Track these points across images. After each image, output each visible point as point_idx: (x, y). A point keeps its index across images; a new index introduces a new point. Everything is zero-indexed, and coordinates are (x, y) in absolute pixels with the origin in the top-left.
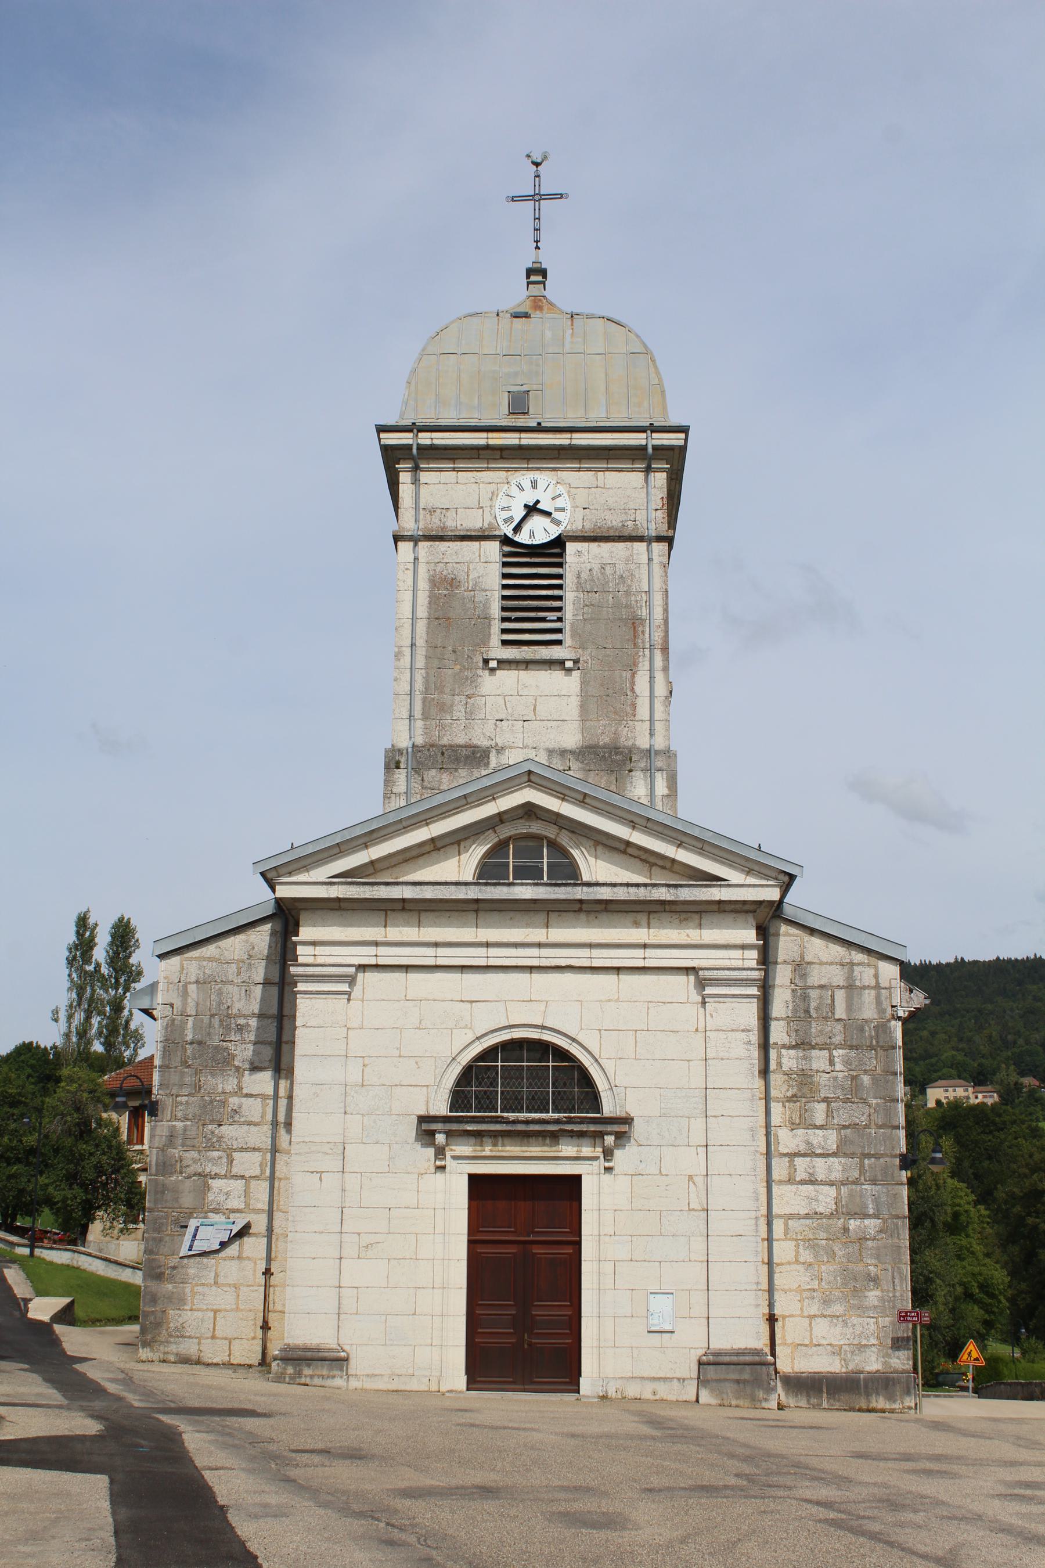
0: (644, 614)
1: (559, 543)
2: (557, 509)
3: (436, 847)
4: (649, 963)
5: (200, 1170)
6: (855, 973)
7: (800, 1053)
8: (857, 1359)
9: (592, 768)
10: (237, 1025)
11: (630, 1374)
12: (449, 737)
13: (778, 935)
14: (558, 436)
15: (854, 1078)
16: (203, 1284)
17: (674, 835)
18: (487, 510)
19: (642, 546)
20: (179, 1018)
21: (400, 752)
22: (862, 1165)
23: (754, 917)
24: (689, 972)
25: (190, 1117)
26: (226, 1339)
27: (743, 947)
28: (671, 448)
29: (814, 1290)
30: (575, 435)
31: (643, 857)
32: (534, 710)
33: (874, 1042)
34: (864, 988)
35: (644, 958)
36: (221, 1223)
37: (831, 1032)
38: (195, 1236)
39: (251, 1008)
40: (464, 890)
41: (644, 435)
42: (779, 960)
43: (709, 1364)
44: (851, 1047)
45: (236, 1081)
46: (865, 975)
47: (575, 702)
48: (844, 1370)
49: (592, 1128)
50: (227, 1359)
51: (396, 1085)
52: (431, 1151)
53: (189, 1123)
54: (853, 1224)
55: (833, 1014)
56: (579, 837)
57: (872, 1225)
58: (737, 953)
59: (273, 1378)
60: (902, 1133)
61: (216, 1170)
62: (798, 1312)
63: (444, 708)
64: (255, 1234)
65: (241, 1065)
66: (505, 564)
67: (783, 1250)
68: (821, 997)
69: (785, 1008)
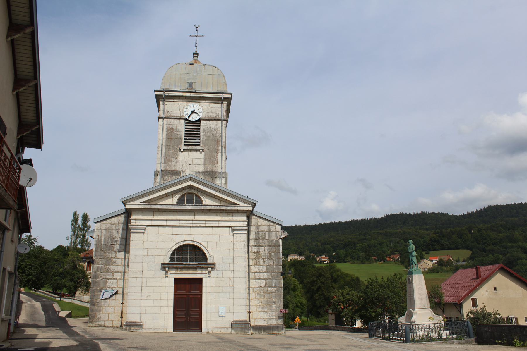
1: (199, 121)
2: (199, 112)
3: (167, 196)
4: (220, 225)
5: (105, 277)
6: (271, 228)
7: (257, 247)
8: (270, 322)
9: (207, 176)
11: (214, 327)
13: (252, 218)
14: (200, 94)
15: (270, 253)
16: (106, 307)
17: (227, 193)
19: (220, 122)
20: (100, 238)
21: (158, 171)
22: (272, 275)
23: (246, 214)
25: (103, 264)
26: (111, 320)
27: (243, 221)
28: (228, 98)
29: (260, 305)
30: (204, 94)
33: (275, 245)
34: (273, 231)
36: (110, 291)
37: (264, 242)
38: (103, 294)
41: (221, 95)
43: (234, 324)
44: (269, 246)
45: (115, 255)
46: (273, 228)
47: (202, 160)
48: (267, 324)
49: (205, 266)
50: (112, 325)
52: (164, 272)
53: (102, 265)
54: (269, 289)
55: (265, 238)
57: (274, 289)
58: (242, 223)
60: (281, 267)
61: (109, 277)
63: (169, 161)
64: (119, 294)
66: (186, 125)
67: (252, 296)
68: (262, 234)
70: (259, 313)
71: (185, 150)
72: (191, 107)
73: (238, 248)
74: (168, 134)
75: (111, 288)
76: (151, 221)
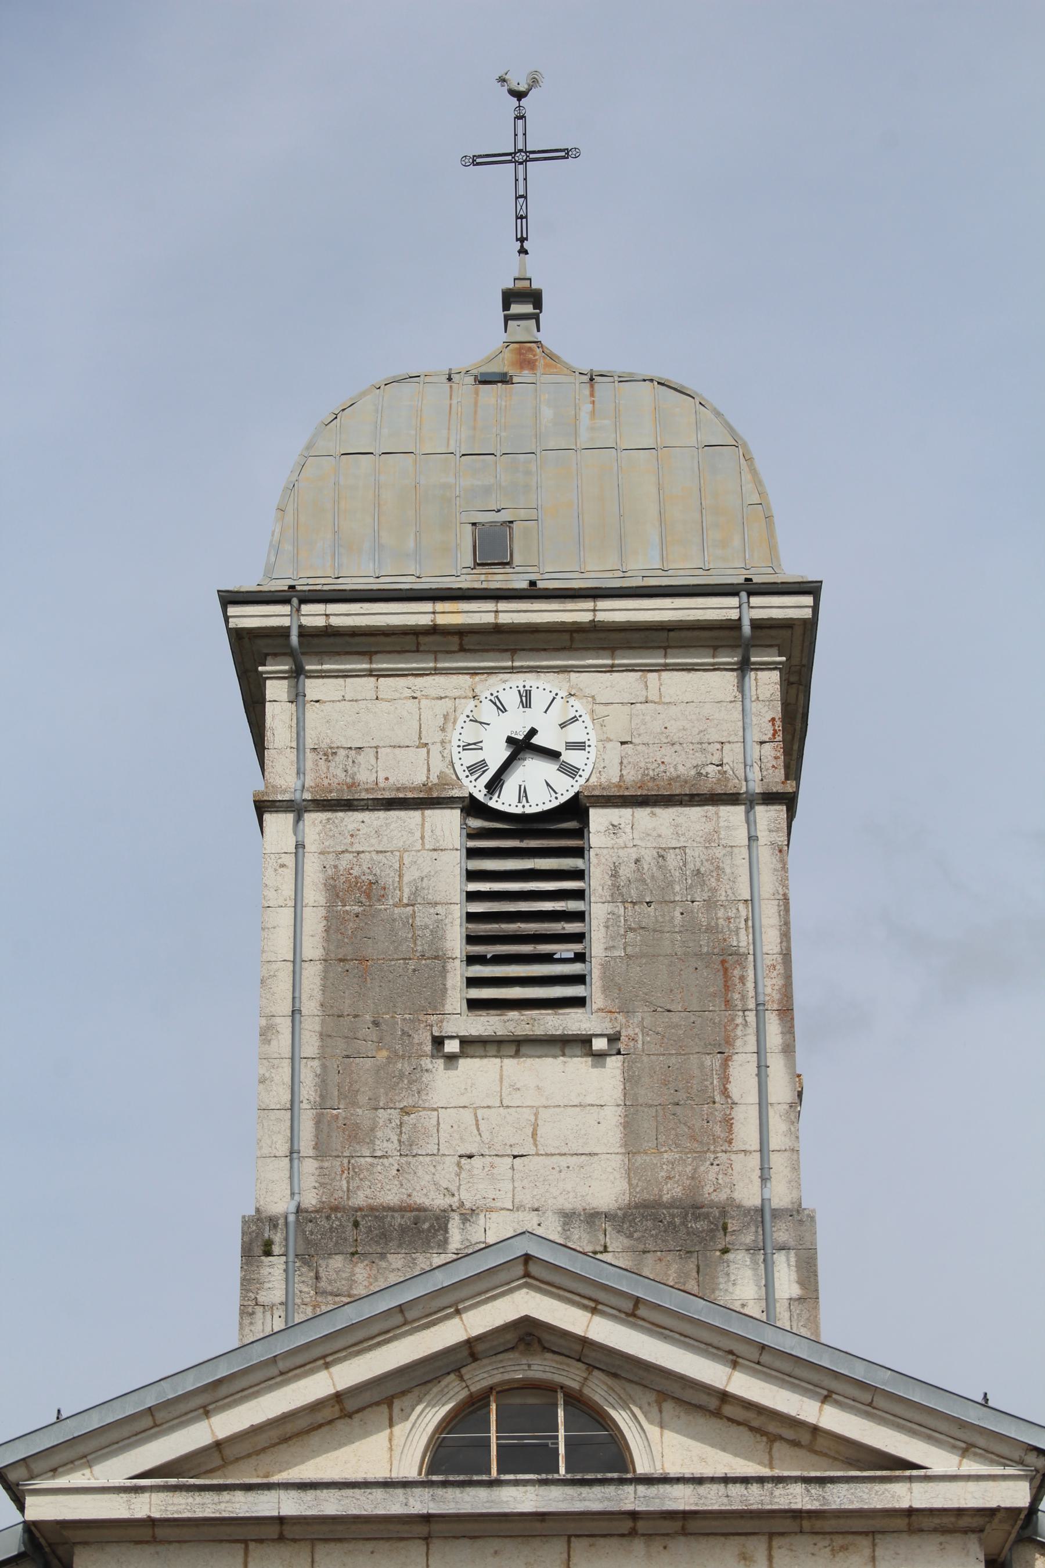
0: (743, 944)
9: (650, 1247)
12: (368, 1192)
14: (570, 605)
17: (814, 1377)
18: (435, 750)
19: (735, 814)
21: (273, 1222)
23: (980, 1540)
28: (787, 625)
30: (602, 604)
31: (755, 1424)
32: (534, 1135)
40: (402, 1498)
41: (734, 601)
47: (612, 1116)
66: (472, 853)
72: (504, 710)
74: (334, 924)
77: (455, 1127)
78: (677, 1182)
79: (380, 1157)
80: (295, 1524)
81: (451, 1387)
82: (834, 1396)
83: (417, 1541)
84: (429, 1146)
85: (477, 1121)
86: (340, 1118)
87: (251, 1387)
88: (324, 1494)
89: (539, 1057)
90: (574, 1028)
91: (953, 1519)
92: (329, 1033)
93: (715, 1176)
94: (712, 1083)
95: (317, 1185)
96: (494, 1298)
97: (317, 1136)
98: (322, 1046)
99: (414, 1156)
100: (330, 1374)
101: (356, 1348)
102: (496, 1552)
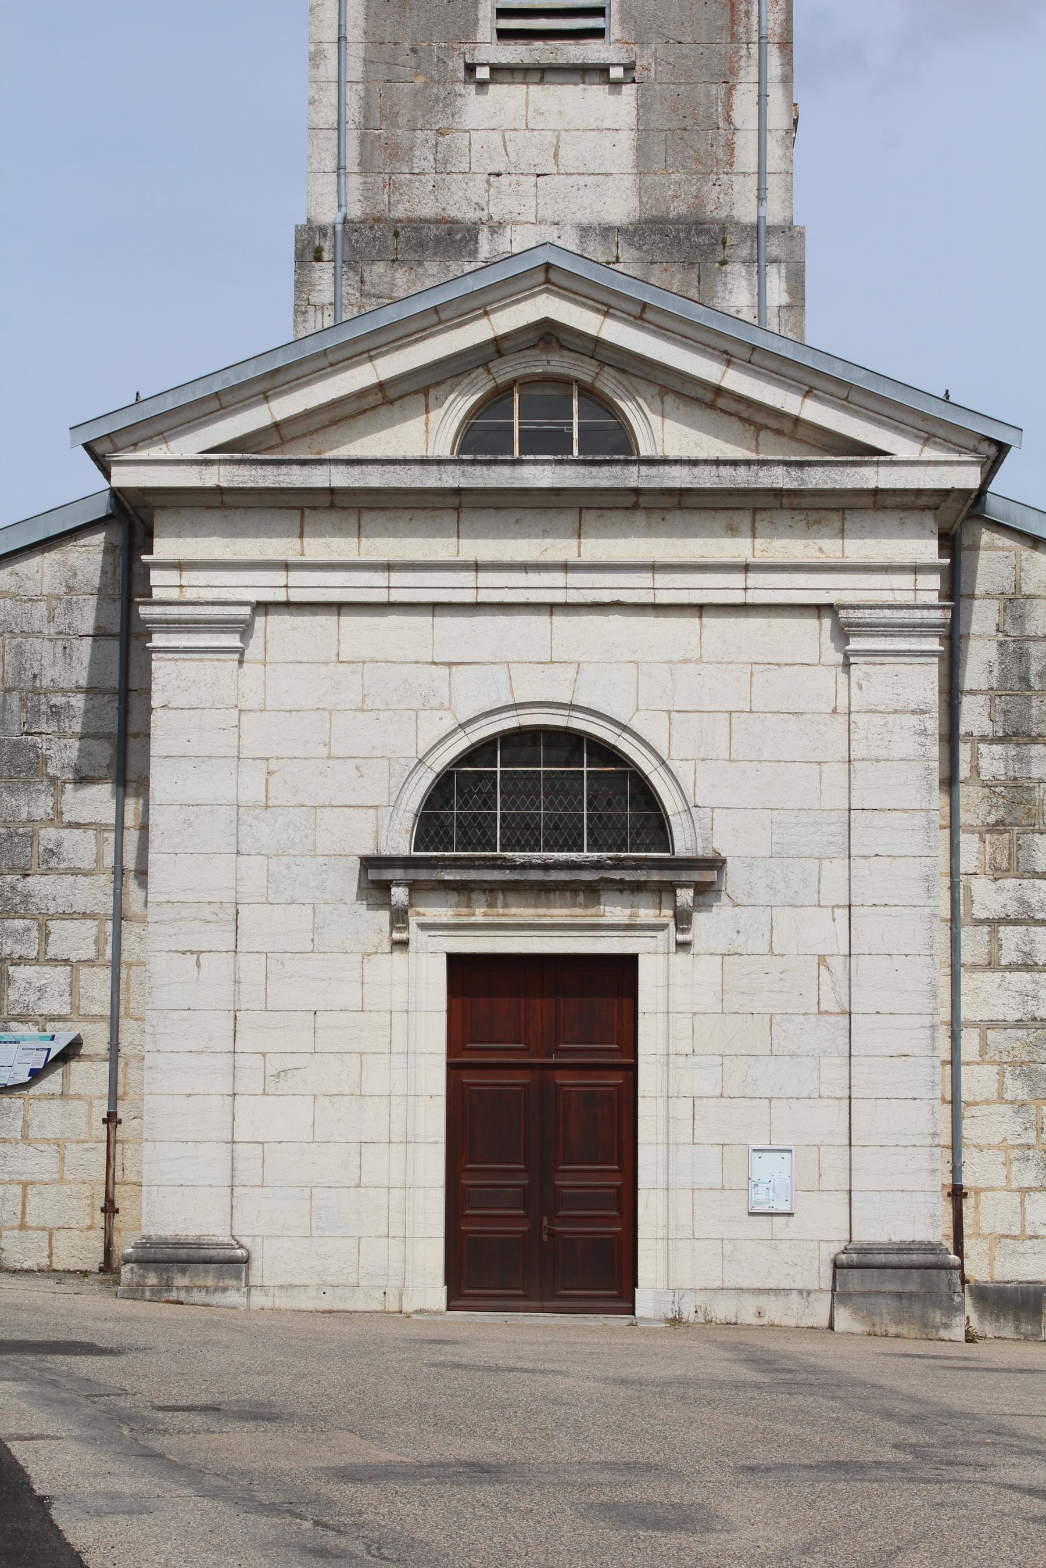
7: (1012, 750)
9: (657, 258)
10: (51, 707)
11: (718, 1284)
12: (407, 205)
13: (975, 548)
17: (798, 374)
21: (322, 231)
23: (935, 516)
24: (823, 612)
26: (43, 1229)
27: (916, 569)
29: (1029, 1147)
31: (745, 415)
32: (556, 155)
35: (746, 589)
36: (32, 1038)
39: (74, 677)
40: (436, 474)
42: (977, 592)
43: (851, 1266)
45: (50, 800)
47: (626, 140)
49: (656, 876)
50: (47, 1261)
51: (323, 806)
52: (383, 916)
56: (635, 381)
58: (905, 580)
59: (124, 1291)
61: (19, 950)
62: (1002, 1183)
63: (396, 153)
64: (89, 1057)
65: (58, 774)
69: (986, 674)
70: (1022, 1201)
71: (501, 72)
73: (883, 753)
75: (36, 1023)
76: (283, 573)
77: (485, 148)
78: (683, 201)
79: (418, 174)
80: (344, 494)
81: (479, 379)
82: (815, 391)
83: (449, 511)
84: (462, 165)
85: (505, 142)
86: (382, 138)
87: (304, 376)
88: (369, 469)
89: (561, 84)
90: (593, 58)
91: (913, 499)
92: (372, 59)
93: (717, 195)
94: (717, 110)
95: (361, 198)
96: (518, 301)
97: (361, 154)
98: (366, 71)
99: (448, 174)
100: (374, 366)
101: (396, 344)
102: (517, 521)
